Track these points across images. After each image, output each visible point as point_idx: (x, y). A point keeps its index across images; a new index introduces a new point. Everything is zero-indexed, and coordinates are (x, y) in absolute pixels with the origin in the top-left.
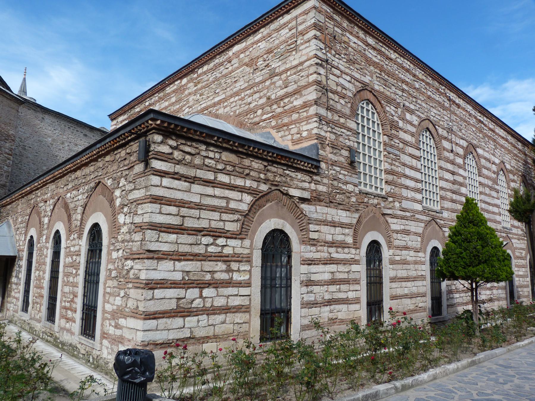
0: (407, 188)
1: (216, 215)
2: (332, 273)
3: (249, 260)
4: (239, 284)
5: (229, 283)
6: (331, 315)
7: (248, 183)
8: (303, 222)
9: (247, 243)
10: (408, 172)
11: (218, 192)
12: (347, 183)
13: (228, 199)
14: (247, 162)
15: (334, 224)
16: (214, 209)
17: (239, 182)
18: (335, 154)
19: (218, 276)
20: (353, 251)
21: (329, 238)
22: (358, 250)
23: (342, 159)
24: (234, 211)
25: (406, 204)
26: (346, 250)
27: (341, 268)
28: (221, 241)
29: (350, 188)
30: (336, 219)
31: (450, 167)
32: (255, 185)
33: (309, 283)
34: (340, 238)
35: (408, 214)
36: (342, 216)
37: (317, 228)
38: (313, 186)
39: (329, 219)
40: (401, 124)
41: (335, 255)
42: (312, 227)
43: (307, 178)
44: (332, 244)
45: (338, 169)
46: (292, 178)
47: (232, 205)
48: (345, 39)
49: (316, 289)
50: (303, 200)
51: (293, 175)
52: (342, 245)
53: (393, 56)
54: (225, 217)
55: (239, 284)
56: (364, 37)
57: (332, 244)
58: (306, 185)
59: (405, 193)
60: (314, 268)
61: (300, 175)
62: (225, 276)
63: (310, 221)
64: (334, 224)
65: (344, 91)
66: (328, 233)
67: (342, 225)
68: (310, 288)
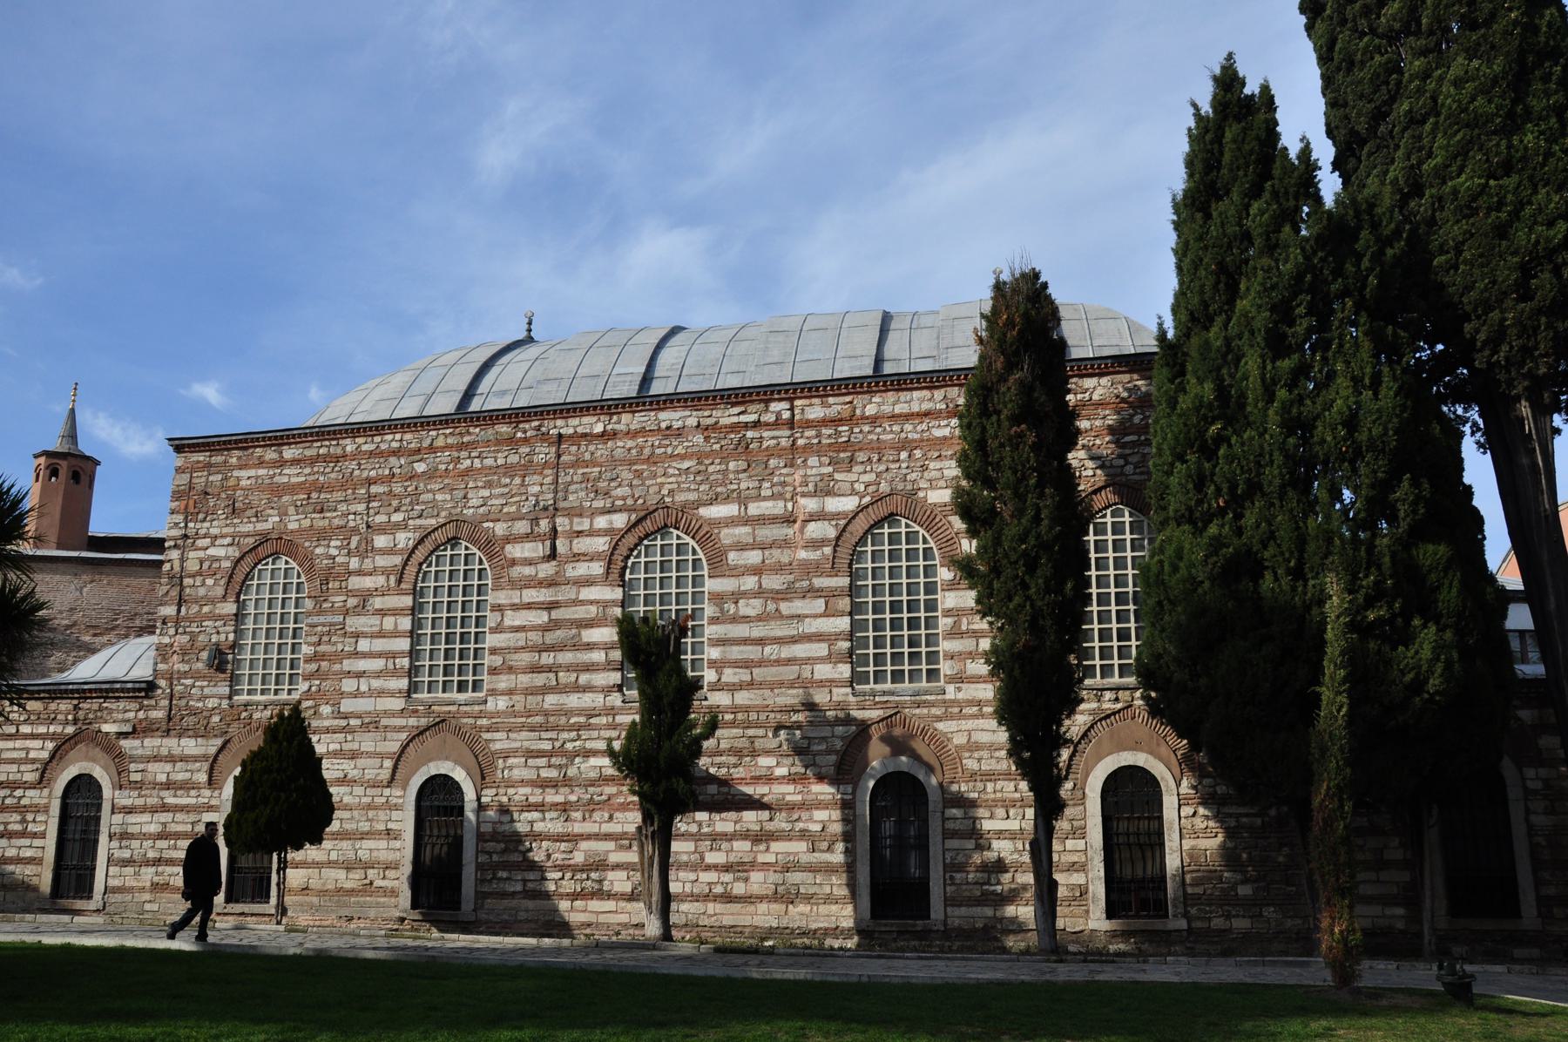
0: (360, 675)
1: (14, 768)
2: (164, 824)
3: (46, 809)
4: (34, 835)
5: (23, 834)
6: (156, 879)
7: (52, 729)
8: (119, 761)
9: (46, 792)
10: (364, 645)
11: (18, 744)
12: (203, 698)
13: (28, 750)
14: (53, 706)
15: (171, 759)
16: (13, 761)
17: (42, 729)
18: (188, 662)
19: (10, 827)
20: (207, 793)
21: (162, 778)
22: (216, 793)
23: (200, 665)
24: (34, 761)
25: (347, 705)
26: (193, 793)
27: (179, 817)
28: (18, 793)
30: (177, 751)
31: (531, 595)
32: (59, 729)
33: (125, 836)
34: (180, 777)
35: (353, 722)
36: (190, 746)
37: (141, 767)
38: (141, 715)
39: (164, 752)
40: (354, 563)
41: (170, 800)
42: (133, 767)
43: (134, 705)
44: (169, 785)
45: (189, 682)
46: (111, 711)
47: (32, 755)
48: (232, 482)
49: (135, 844)
50: (124, 735)
51: (114, 706)
52: (186, 786)
53: (349, 446)
54: (23, 768)
55: (34, 835)
56: (274, 456)
57: (169, 785)
58: (131, 715)
59: (349, 685)
60: (132, 819)
61: (122, 704)
62: (18, 827)
63: (133, 759)
64: (171, 759)
65: (216, 565)
66: (160, 772)
67: (184, 759)
68: (124, 843)
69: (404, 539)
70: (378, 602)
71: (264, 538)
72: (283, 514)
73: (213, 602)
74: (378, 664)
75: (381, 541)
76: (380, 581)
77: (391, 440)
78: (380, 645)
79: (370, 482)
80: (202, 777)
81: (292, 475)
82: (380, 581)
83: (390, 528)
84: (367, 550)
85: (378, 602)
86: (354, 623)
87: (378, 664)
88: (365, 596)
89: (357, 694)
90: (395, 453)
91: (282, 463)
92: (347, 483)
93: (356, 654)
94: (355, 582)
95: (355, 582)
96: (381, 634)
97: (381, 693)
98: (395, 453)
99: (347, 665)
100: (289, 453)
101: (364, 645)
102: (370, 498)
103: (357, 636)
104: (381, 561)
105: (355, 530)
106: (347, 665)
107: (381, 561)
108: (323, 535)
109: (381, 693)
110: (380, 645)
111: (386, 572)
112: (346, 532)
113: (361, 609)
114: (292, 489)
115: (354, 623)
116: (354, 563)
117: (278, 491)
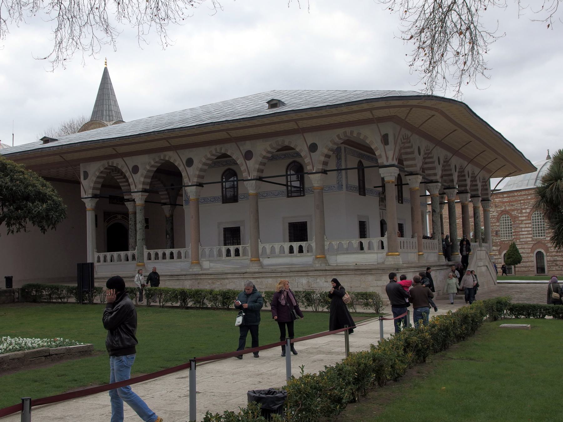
0: (523, 235)
10: (523, 229)
29: (497, 241)
59: (521, 236)
69: (528, 211)
70: (525, 222)
71: (502, 211)
72: (505, 206)
73: (495, 223)
74: (526, 233)
75: (524, 211)
76: (525, 218)
77: (523, 193)
78: (526, 229)
79: (520, 200)
80: (497, 253)
81: (506, 200)
82: (525, 218)
83: (525, 209)
84: (521, 213)
85: (525, 222)
86: (521, 226)
87: (526, 233)
88: (522, 221)
89: (523, 238)
90: (525, 195)
91: (504, 197)
92: (516, 201)
93: (522, 231)
94: (520, 219)
95: (520, 219)
96: (526, 227)
97: (528, 238)
98: (525, 195)
99: (521, 233)
100: (505, 196)
101: (523, 229)
102: (521, 203)
103: (522, 228)
104: (524, 215)
105: (519, 209)
106: (521, 233)
107: (524, 215)
108: (513, 210)
109: (528, 238)
110: (526, 229)
111: (526, 216)
112: (517, 210)
113: (521, 224)
114: (506, 202)
115: (521, 226)
116: (520, 215)
117: (504, 203)
